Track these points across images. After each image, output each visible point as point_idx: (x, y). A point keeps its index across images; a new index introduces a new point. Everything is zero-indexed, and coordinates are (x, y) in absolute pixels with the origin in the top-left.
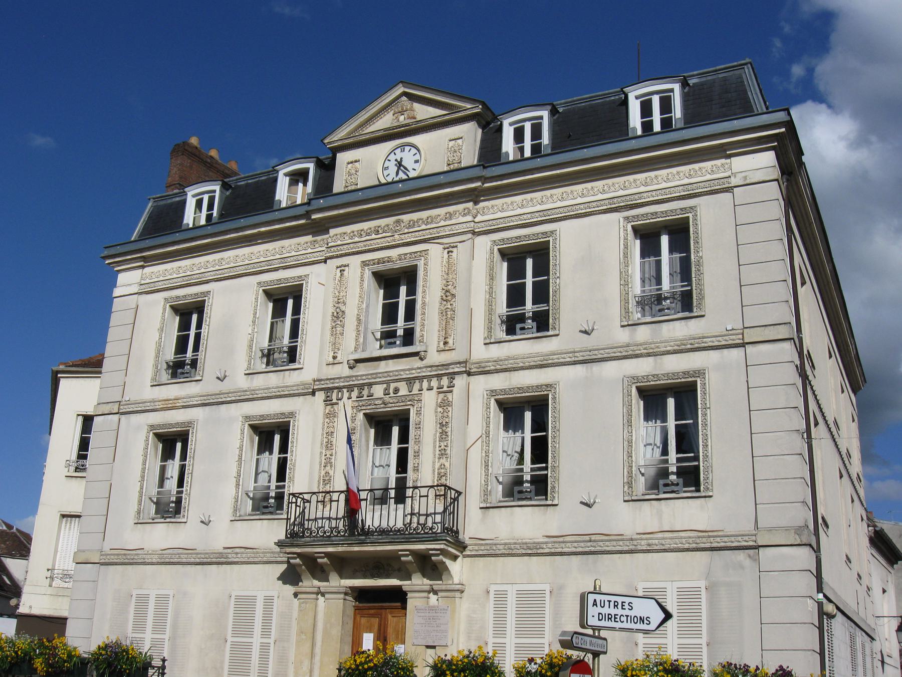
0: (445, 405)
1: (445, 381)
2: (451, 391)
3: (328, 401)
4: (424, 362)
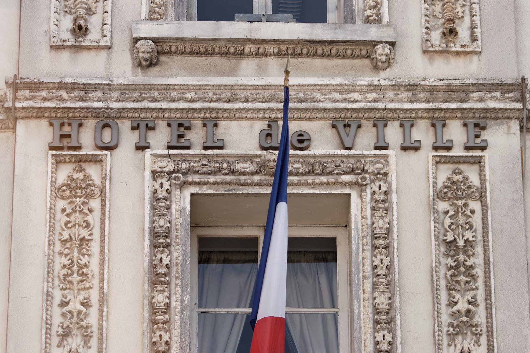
0: (454, 192)
1: (456, 133)
2: (478, 161)
3: (63, 146)
4: (383, 74)
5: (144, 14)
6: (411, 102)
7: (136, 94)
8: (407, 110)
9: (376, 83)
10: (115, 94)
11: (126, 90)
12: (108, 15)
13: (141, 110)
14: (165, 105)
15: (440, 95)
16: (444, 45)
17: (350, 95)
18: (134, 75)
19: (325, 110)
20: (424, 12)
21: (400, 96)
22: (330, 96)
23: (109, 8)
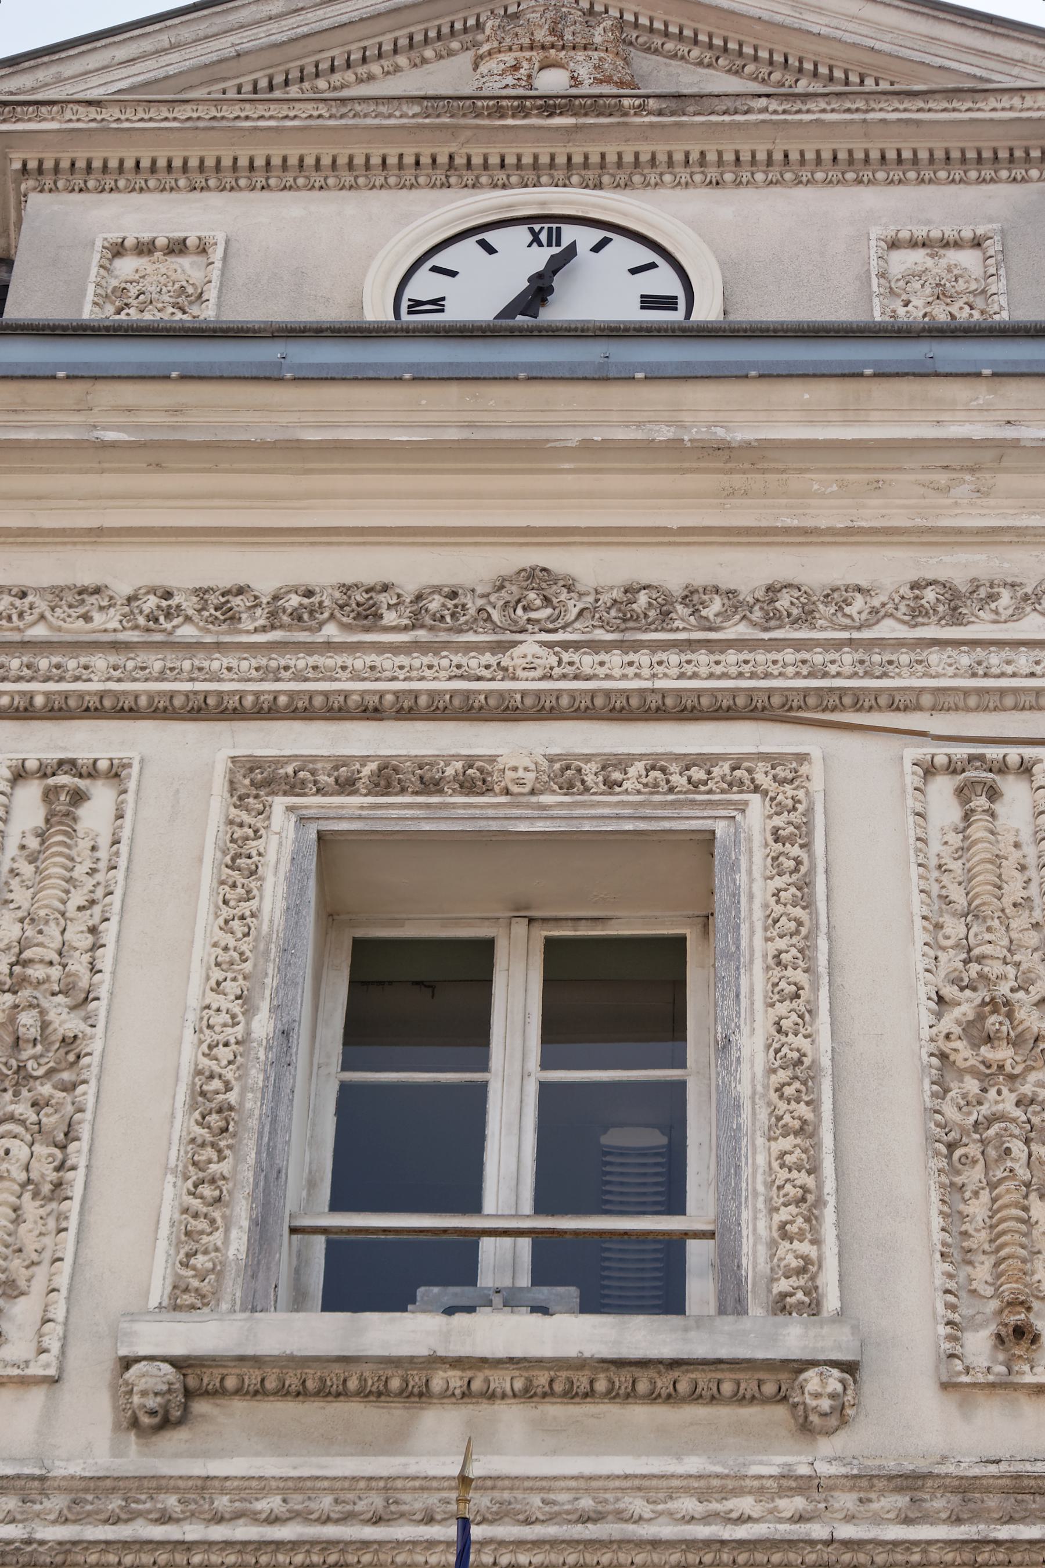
4: (826, 1446)
5: (158, 1292)
6: (907, 1521)
7: (115, 1504)
8: (895, 1544)
9: (804, 1470)
10: (57, 1503)
11: (87, 1493)
12: (61, 1298)
13: (126, 1545)
14: (193, 1532)
15: (992, 1502)
16: (1002, 1369)
17: (729, 1504)
18: (117, 1452)
19: (655, 1544)
20: (940, 1281)
21: (875, 1506)
22: (671, 1505)
23: (62, 1281)
